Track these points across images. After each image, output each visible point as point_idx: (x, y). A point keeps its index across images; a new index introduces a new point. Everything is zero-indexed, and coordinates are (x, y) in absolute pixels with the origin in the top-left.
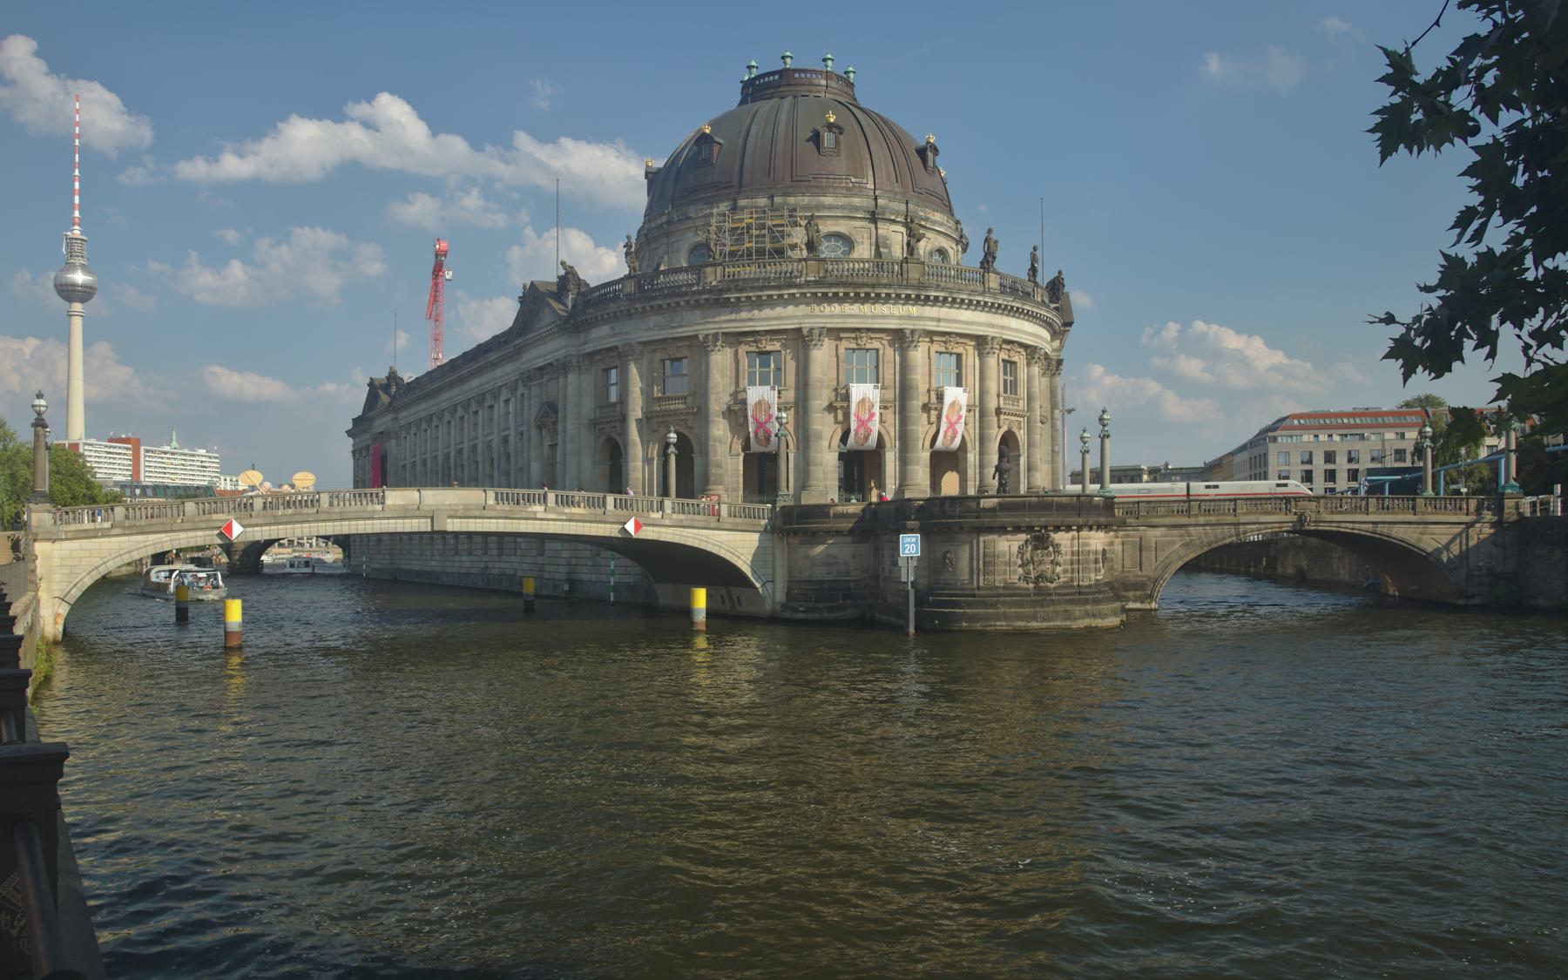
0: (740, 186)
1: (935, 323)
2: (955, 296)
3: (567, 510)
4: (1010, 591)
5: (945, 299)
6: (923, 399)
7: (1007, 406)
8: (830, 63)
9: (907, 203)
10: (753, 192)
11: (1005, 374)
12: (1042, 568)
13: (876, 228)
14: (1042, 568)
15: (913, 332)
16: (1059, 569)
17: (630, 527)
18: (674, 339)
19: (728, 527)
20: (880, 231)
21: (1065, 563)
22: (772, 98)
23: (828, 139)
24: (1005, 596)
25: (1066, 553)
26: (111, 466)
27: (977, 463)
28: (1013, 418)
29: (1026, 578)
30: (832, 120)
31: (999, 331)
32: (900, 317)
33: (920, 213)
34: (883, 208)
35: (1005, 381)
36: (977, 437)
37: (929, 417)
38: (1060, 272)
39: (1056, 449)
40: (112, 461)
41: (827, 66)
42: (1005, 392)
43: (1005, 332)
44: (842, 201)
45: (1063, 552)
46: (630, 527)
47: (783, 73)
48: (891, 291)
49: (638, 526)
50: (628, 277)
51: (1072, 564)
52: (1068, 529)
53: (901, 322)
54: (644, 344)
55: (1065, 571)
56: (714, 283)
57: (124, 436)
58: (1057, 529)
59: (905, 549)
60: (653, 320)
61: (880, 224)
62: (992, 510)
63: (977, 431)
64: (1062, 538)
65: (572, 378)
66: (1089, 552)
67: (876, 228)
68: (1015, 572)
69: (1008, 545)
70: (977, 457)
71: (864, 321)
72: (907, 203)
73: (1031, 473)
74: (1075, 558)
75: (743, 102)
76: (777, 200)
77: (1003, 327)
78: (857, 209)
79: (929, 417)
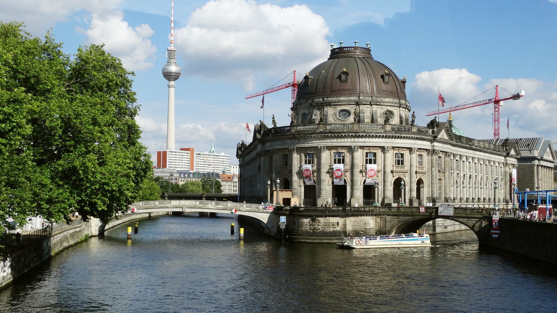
0: (315, 94)
1: (363, 143)
2: (370, 134)
3: (217, 206)
4: (307, 232)
5: (366, 135)
6: (361, 168)
7: (398, 169)
8: (357, 43)
9: (372, 97)
10: (319, 96)
11: (396, 158)
12: (315, 226)
13: (359, 107)
14: (315, 226)
15: (355, 147)
16: (319, 227)
17: (233, 211)
18: (284, 148)
19: (261, 212)
20: (360, 108)
21: (322, 225)
22: (335, 58)
23: (343, 77)
24: (305, 233)
25: (322, 223)
26: (181, 161)
27: (383, 189)
28: (400, 173)
29: (310, 229)
30: (345, 70)
31: (391, 144)
32: (350, 142)
33: (378, 100)
34: (362, 100)
35: (396, 160)
36: (383, 180)
37: (362, 175)
38: (436, 117)
39: (433, 182)
40: (181, 159)
41: (356, 45)
42: (396, 164)
43: (393, 144)
44: (346, 98)
45: (321, 222)
46: (233, 211)
47: (340, 48)
48: (346, 134)
49: (236, 211)
50: (273, 128)
51: (324, 225)
52: (322, 217)
53: (351, 143)
54: (277, 149)
55: (322, 227)
56: (293, 132)
57: (187, 147)
58: (319, 216)
59: (281, 220)
60: (279, 142)
61: (360, 106)
62: (302, 211)
63: (383, 178)
64: (322, 220)
65: (262, 158)
66: (330, 223)
67: (359, 107)
68: (308, 227)
69: (306, 221)
70: (383, 187)
71: (338, 144)
72: (372, 97)
73: (411, 192)
74: (325, 224)
75: (329, 59)
76: (325, 99)
77: (393, 143)
78: (352, 101)
79: (362, 175)
